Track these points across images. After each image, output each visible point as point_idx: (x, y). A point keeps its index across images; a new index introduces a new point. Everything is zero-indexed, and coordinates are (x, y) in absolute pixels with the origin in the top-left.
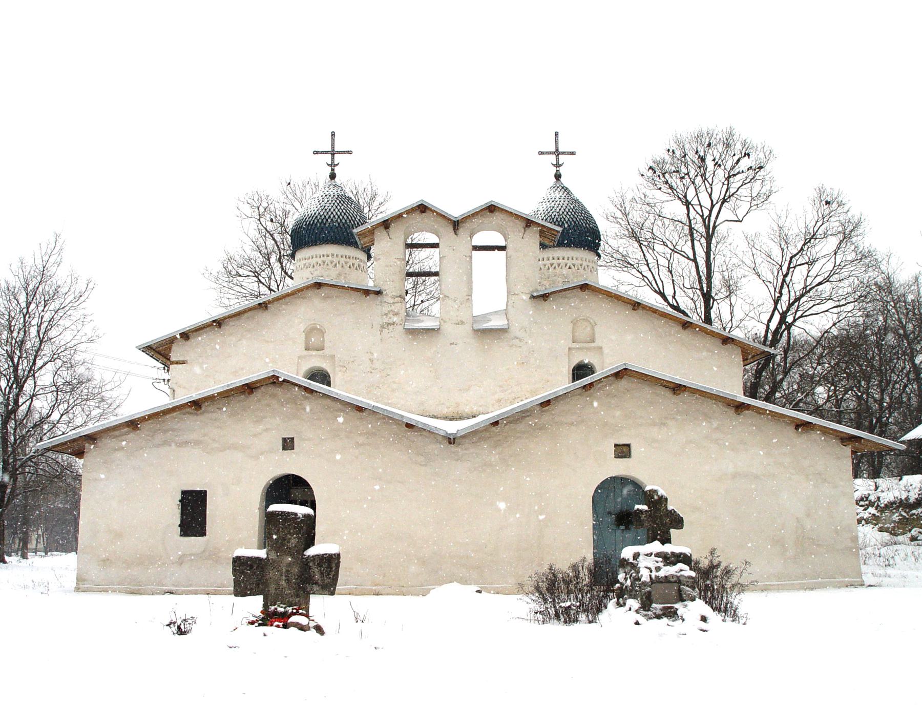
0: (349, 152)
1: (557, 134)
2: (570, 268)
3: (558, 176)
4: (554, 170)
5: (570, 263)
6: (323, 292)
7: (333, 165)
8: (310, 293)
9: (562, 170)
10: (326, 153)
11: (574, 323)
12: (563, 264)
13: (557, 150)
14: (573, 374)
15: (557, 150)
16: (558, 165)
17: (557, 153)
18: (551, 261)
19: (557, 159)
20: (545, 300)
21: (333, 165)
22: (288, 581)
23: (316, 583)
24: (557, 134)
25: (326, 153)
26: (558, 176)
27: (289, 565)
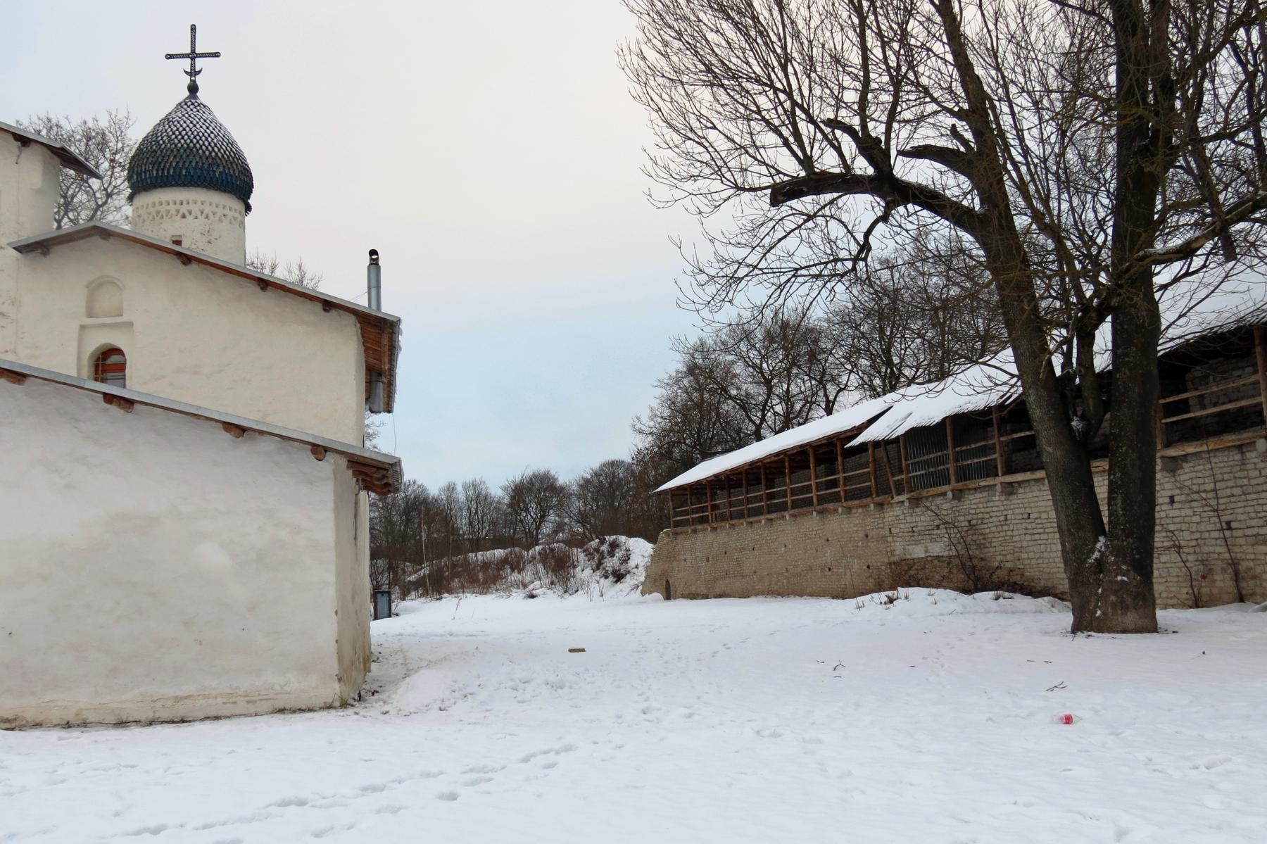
1: (193, 28)
2: (184, 217)
3: (193, 89)
4: (187, 79)
5: (184, 209)
9: (198, 79)
11: (94, 288)
12: (173, 212)
13: (193, 50)
14: (97, 366)
15: (193, 50)
16: (193, 73)
17: (193, 56)
18: (158, 208)
19: (193, 65)
24: (193, 28)
26: (193, 89)
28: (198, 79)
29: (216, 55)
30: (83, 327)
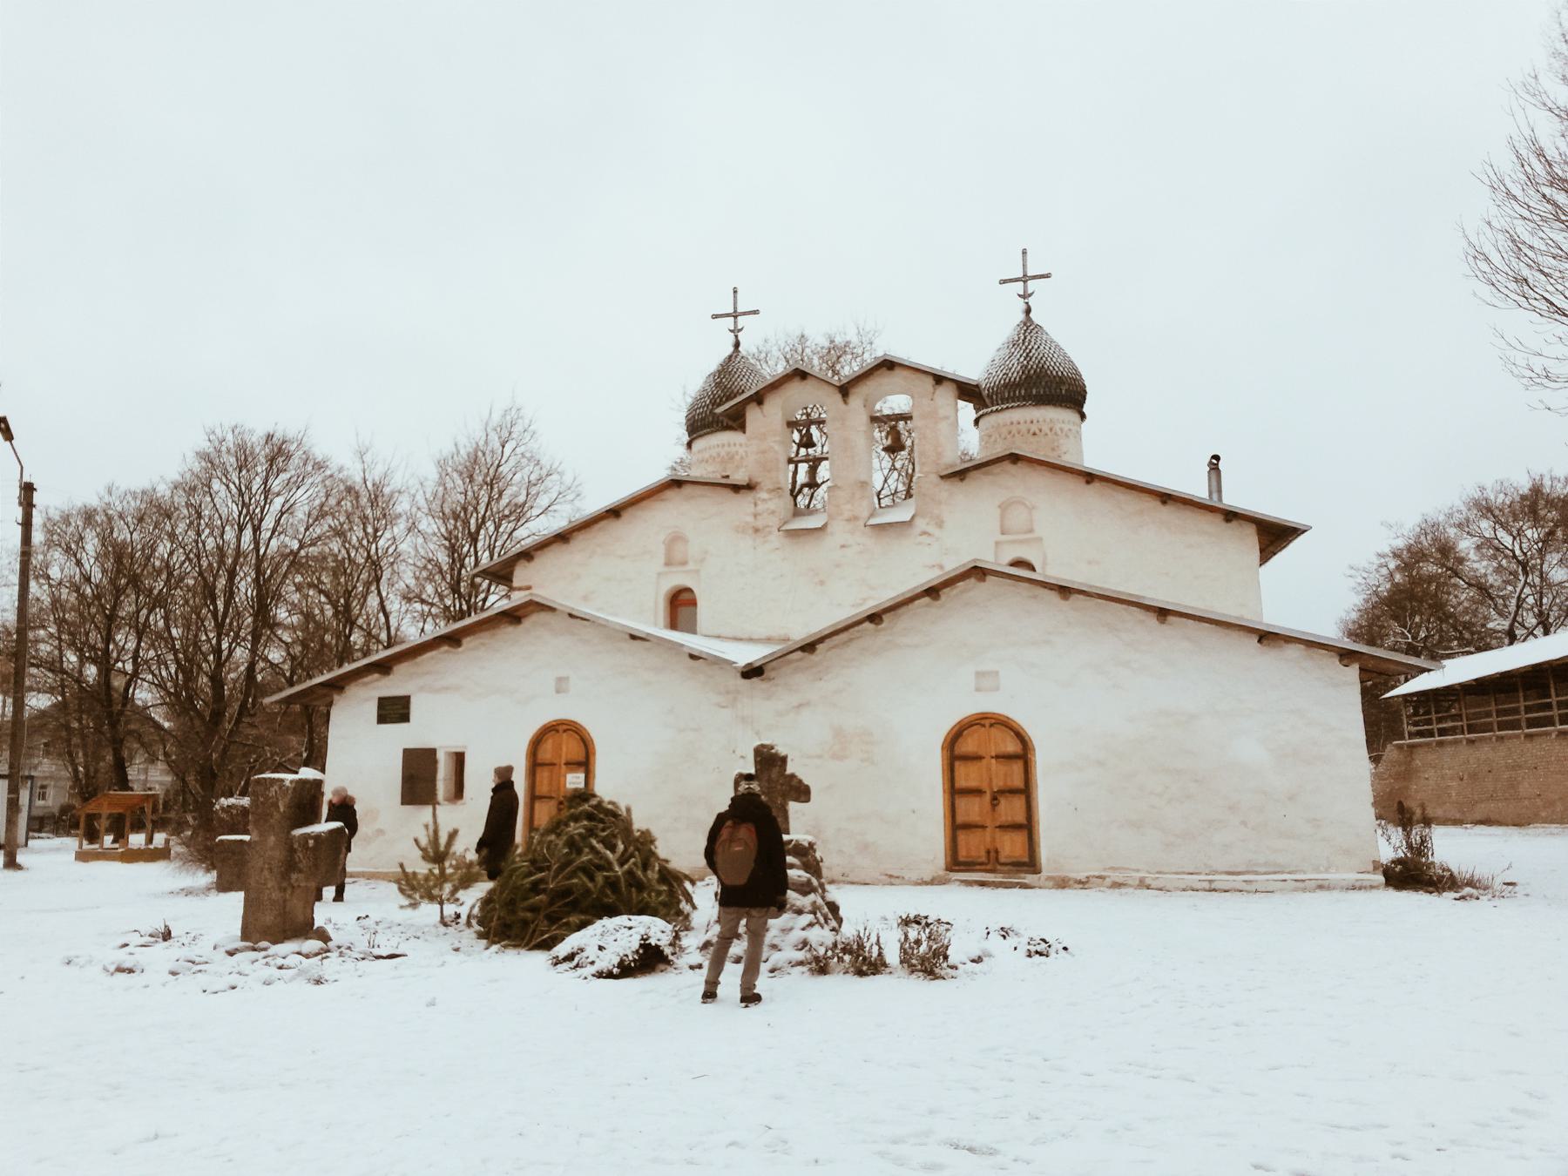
0: (756, 312)
1: (1024, 252)
5: (1034, 428)
6: (687, 490)
7: (736, 331)
8: (670, 494)
9: (1031, 300)
10: (728, 315)
11: (1004, 508)
20: (1088, 482)
21: (736, 331)
22: (271, 870)
23: (300, 871)
24: (1024, 252)
25: (728, 315)
27: (272, 849)
28: (1031, 300)
29: (1047, 276)
30: (997, 543)
